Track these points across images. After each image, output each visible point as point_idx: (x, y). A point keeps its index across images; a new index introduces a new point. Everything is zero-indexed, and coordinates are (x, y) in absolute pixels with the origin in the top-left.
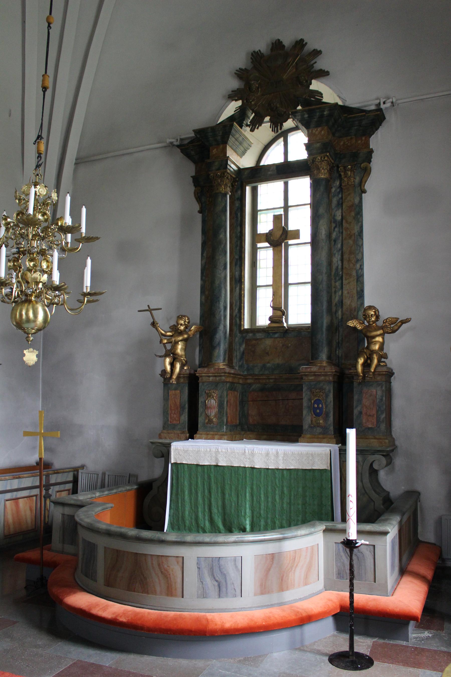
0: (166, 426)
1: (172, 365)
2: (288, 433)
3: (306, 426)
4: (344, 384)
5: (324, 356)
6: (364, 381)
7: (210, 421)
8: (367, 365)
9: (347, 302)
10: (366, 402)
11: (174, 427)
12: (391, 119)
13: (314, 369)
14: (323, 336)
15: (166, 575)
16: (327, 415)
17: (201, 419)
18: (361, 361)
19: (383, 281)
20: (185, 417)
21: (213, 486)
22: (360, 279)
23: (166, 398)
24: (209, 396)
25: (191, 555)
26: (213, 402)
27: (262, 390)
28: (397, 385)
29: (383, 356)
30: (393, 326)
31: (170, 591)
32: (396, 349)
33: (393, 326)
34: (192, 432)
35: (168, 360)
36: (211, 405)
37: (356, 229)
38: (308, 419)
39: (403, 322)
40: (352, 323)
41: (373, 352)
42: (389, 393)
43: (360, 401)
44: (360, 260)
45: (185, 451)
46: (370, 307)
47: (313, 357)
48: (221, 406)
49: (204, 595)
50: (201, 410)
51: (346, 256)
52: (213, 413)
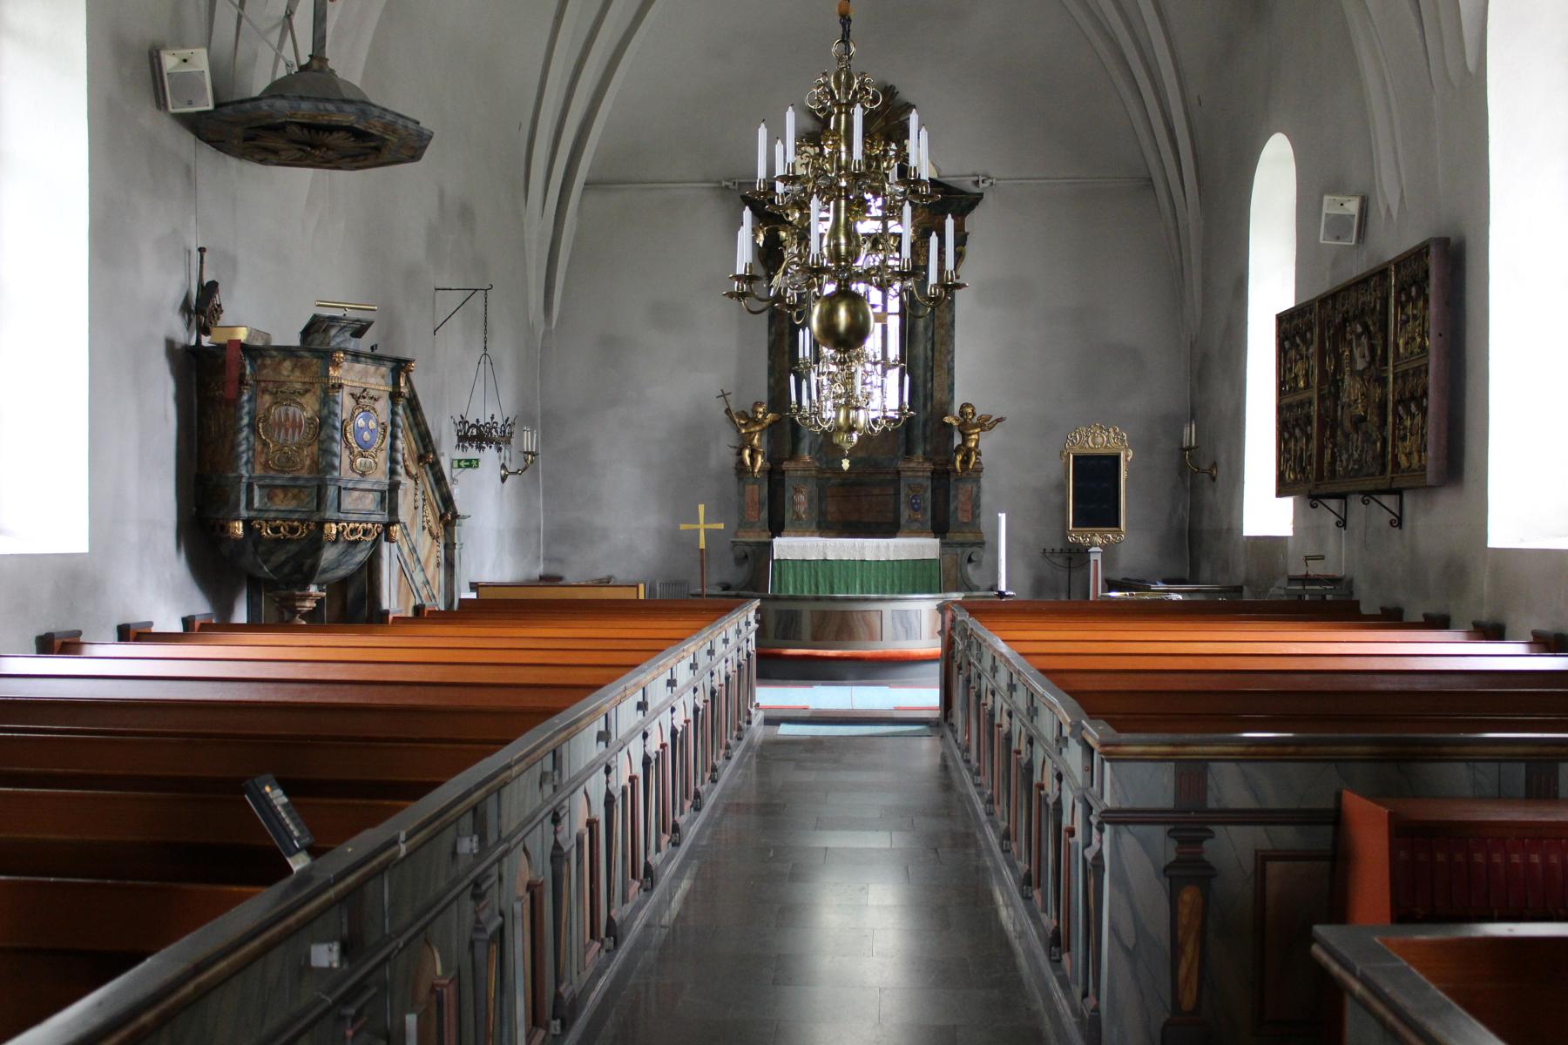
0: (744, 524)
1: (751, 456)
2: (889, 529)
3: (903, 521)
4: (943, 478)
5: (920, 452)
6: (958, 480)
7: (799, 518)
8: (965, 462)
9: (937, 395)
10: (962, 498)
11: (752, 525)
12: (988, 198)
13: (912, 465)
14: (918, 432)
15: (868, 625)
16: (925, 509)
17: (788, 516)
18: (959, 458)
19: (972, 379)
20: (765, 515)
21: (821, 580)
22: (951, 370)
23: (741, 494)
24: (797, 491)
25: (887, 608)
26: (802, 498)
27: (842, 485)
28: (985, 482)
29: (979, 454)
30: (985, 424)
31: (872, 637)
32: (986, 444)
33: (985, 424)
34: (777, 529)
35: (747, 452)
36: (800, 501)
37: (948, 318)
38: (905, 513)
39: (999, 420)
40: (947, 420)
41: (970, 450)
42: (979, 488)
43: (956, 496)
44: (951, 352)
45: (786, 547)
46: (968, 405)
47: (909, 452)
48: (810, 500)
49: (896, 638)
50: (787, 506)
51: (937, 346)
52: (802, 509)
